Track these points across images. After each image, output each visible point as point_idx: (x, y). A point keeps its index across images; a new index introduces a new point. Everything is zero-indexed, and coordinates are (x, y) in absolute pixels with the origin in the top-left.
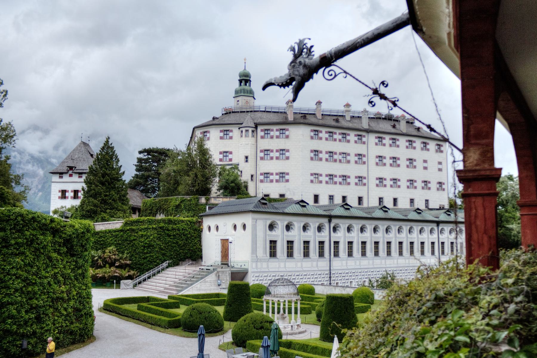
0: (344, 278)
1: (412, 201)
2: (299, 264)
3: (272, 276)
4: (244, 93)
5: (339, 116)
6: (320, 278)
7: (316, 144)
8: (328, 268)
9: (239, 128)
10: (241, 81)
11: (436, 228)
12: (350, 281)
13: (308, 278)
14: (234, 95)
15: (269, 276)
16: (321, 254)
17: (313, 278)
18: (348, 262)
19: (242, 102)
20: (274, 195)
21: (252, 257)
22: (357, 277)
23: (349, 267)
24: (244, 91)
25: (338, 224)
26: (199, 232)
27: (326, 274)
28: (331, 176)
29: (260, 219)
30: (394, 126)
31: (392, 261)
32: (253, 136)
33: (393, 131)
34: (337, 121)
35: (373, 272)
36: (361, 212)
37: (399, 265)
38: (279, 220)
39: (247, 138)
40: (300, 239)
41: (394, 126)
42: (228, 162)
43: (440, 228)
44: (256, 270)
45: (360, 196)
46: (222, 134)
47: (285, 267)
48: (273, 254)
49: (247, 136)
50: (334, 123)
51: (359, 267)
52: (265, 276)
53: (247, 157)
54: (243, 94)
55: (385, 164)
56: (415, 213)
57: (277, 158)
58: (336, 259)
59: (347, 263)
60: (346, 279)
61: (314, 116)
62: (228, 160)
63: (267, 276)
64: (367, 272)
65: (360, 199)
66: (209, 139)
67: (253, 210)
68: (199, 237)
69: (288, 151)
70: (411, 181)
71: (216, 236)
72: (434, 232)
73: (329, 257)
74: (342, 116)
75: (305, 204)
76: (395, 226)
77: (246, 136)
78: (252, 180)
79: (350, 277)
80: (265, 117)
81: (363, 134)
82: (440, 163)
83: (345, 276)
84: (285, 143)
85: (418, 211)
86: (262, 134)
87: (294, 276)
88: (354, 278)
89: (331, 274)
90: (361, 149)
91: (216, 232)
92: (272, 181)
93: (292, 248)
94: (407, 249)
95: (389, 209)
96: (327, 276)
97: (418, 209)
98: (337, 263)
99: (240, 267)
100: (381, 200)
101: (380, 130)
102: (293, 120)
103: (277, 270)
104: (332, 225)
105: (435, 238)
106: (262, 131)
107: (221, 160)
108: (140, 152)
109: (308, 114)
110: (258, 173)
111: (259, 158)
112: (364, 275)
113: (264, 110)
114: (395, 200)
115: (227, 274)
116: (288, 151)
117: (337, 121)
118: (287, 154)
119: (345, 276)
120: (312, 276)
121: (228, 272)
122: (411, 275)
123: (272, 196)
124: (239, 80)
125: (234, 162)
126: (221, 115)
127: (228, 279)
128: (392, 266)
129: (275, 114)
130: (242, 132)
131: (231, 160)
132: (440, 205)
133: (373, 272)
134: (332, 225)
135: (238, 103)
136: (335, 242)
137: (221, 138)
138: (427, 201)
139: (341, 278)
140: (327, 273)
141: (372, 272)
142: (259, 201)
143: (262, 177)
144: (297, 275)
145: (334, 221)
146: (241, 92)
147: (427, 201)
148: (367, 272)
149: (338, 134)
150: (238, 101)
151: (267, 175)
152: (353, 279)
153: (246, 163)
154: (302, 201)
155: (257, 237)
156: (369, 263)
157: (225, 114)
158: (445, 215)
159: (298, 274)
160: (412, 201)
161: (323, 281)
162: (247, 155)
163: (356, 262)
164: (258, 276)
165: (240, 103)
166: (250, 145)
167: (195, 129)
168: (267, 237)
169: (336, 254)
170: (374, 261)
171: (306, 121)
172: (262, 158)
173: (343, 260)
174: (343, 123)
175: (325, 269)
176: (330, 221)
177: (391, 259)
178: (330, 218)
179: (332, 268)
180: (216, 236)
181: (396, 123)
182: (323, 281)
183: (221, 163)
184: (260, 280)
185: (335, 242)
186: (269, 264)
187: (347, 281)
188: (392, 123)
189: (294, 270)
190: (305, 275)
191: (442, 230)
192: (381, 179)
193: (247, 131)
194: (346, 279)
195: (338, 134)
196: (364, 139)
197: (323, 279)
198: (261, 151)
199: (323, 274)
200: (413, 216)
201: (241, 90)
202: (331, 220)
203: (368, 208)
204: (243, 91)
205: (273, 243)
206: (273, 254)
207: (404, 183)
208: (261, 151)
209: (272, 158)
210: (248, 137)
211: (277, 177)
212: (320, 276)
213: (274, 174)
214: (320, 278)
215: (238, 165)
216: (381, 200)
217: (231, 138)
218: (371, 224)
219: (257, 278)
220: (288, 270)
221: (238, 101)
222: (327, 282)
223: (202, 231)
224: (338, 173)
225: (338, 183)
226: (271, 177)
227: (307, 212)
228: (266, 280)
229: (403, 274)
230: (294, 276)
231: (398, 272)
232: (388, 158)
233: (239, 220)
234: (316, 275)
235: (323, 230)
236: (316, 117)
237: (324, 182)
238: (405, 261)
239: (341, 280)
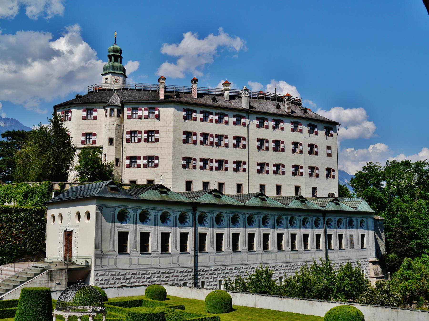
0: (211, 276)
1: (297, 189)
2: (156, 260)
3: (120, 274)
4: (113, 70)
5: (218, 95)
6: (181, 276)
7: (190, 126)
8: (192, 265)
9: (104, 108)
10: (110, 57)
11: (321, 218)
12: (218, 279)
13: (167, 277)
14: (103, 73)
15: (117, 274)
17: (172, 277)
18: (216, 257)
19: (111, 79)
20: (142, 181)
21: (96, 252)
22: (227, 275)
23: (218, 264)
24: (113, 67)
25: (205, 213)
26: (43, 223)
27: (189, 272)
28: (205, 161)
29: (106, 207)
30: (278, 107)
31: (270, 255)
32: (118, 116)
33: (276, 111)
34: (214, 100)
35: (246, 268)
36: (233, 200)
37: (278, 261)
39: (111, 118)
41: (278, 107)
42: (91, 144)
43: (326, 218)
44: (101, 268)
45: (239, 182)
46: (85, 114)
47: (138, 264)
49: (113, 115)
50: (210, 102)
51: (230, 263)
52: (112, 275)
53: (111, 140)
54: (112, 71)
55: (267, 149)
56: (298, 202)
57: (146, 141)
58: (201, 254)
59: (215, 259)
60: (214, 278)
61: (189, 95)
62: (91, 142)
63: (114, 275)
64: (239, 269)
65: (239, 187)
66: (70, 119)
67: (97, 195)
68: (43, 230)
69: (157, 132)
70: (296, 168)
71: (60, 227)
72: (320, 223)
73: (193, 252)
74: (221, 95)
75: (165, 190)
76: (273, 215)
77: (111, 115)
78: (117, 164)
79: (219, 275)
80: (133, 96)
81: (244, 114)
82: (329, 148)
83: (212, 274)
84: (154, 124)
85: (302, 200)
86: (129, 113)
87: (149, 274)
88: (224, 275)
90: (240, 131)
91: (60, 223)
92: (139, 166)
93: (147, 241)
94: (287, 242)
95: (267, 197)
96: (190, 273)
97: (301, 197)
99: (80, 264)
100: (262, 187)
101: (262, 110)
102: (164, 98)
103: (127, 267)
104: (197, 215)
106: (128, 110)
107: (83, 143)
108: (4, 136)
109: (182, 93)
110: (124, 157)
111: (125, 141)
112: (235, 272)
113: (134, 88)
114: (279, 188)
115: (63, 273)
116: (157, 132)
117: (214, 100)
118: (157, 136)
119: (212, 274)
120: (172, 274)
121: (64, 271)
122: (292, 272)
123: (139, 182)
124: (108, 56)
125: (97, 145)
126: (87, 93)
127: (64, 279)
128: (270, 261)
129: (146, 92)
130: (107, 110)
131: (94, 142)
132: (329, 194)
133: (246, 268)
134: (197, 215)
135: (107, 80)
137: (85, 118)
138: (314, 189)
139: (207, 276)
140: (191, 270)
141: (245, 268)
142: (107, 185)
143: (128, 162)
144: (153, 273)
145: (201, 210)
146: (110, 69)
147: (314, 189)
148: (239, 269)
149: (214, 114)
150: (107, 79)
151: (133, 159)
152: (222, 277)
153: (111, 146)
154: (162, 186)
155: (103, 228)
156: (242, 258)
157: (91, 92)
158: (333, 203)
159: (154, 272)
160: (297, 189)
161: (186, 280)
162: (111, 136)
164: (103, 275)
165: (109, 81)
166: (115, 125)
167: (56, 109)
168: (116, 228)
170: (248, 256)
171: (179, 100)
172: (129, 141)
173: (210, 255)
174: (221, 102)
176: (194, 211)
178: (195, 206)
180: (60, 227)
181: (280, 104)
182: (186, 280)
183: (83, 146)
184: (106, 280)
186: (118, 260)
187: (215, 279)
188: (275, 103)
189: (149, 266)
190: (162, 273)
191: (329, 220)
192: (262, 165)
193: (112, 110)
194: (214, 278)
195: (214, 114)
196: (243, 120)
197: (185, 278)
198: (128, 133)
199: (186, 272)
200: (296, 205)
201: (110, 67)
203: (245, 195)
204: (111, 68)
206: (122, 248)
207: (289, 170)
208: (128, 133)
209: (139, 141)
210: (114, 117)
211: (145, 162)
212: (181, 274)
213: (142, 158)
214: (181, 276)
215: (102, 148)
216: (262, 187)
217: (95, 118)
218: (245, 214)
219: (101, 277)
220: (141, 267)
221: (107, 79)
222: (190, 281)
223: (46, 222)
224: (214, 158)
225: (214, 168)
226: (139, 162)
227: (166, 199)
228: (113, 279)
229: (283, 271)
230: (149, 274)
231: (277, 268)
232: (270, 141)
233: (82, 209)
234: (177, 273)
235: (187, 220)
236: (191, 96)
237: (198, 167)
238: (286, 256)
239: (208, 278)
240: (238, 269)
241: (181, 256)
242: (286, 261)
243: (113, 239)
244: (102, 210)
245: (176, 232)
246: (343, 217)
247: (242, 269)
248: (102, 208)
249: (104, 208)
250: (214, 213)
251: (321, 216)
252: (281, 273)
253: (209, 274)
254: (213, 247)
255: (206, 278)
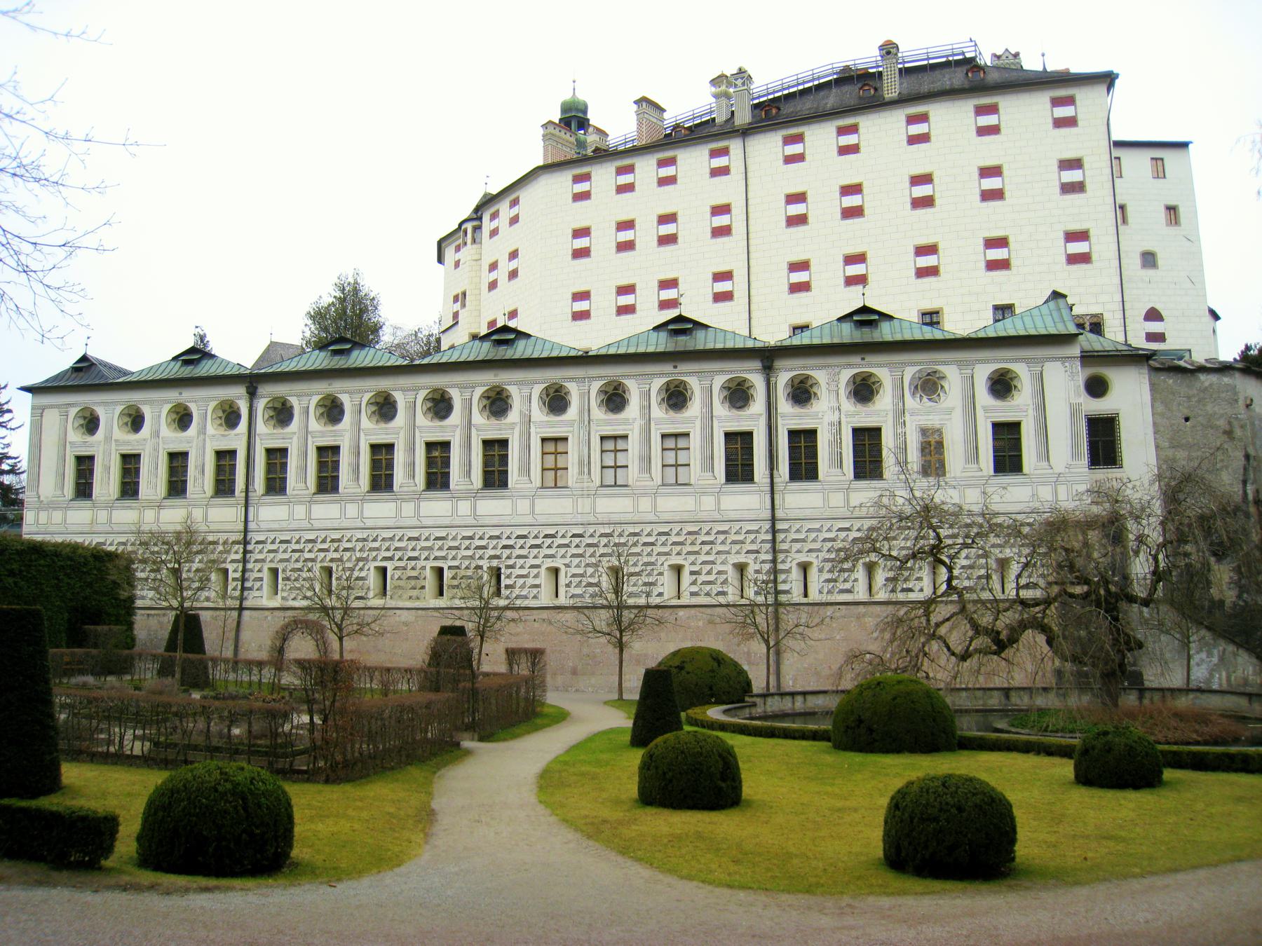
8: (241, 527)
11: (757, 381)
16: (224, 487)
23: (317, 524)
29: (51, 407)
38: (99, 404)
40: (156, 450)
48: (84, 489)
73: (244, 494)
89: (254, 541)
98: (270, 513)
105: (755, 417)
136: (270, 452)
145: (268, 392)
163: (343, 511)
169: (276, 485)
175: (228, 527)
177: (503, 498)
179: (252, 526)
185: (270, 452)
202: (256, 388)
205: (85, 464)
222: (235, 565)
240: (384, 539)
241: (214, 506)
242: (574, 521)
243: (62, 471)
244: (42, 413)
245: (204, 448)
246: (880, 366)
247: (399, 540)
248: (43, 410)
249: (46, 411)
250: (311, 395)
251: (756, 371)
252: (552, 556)
253: (290, 550)
254: (306, 483)
255: (281, 561)
